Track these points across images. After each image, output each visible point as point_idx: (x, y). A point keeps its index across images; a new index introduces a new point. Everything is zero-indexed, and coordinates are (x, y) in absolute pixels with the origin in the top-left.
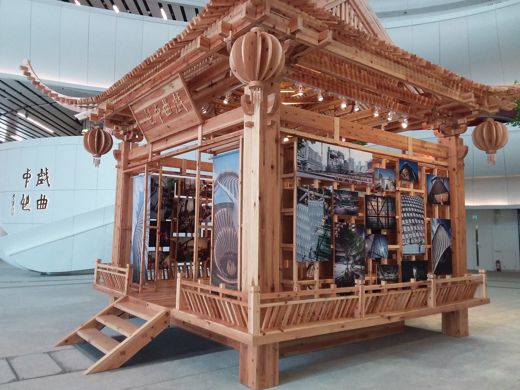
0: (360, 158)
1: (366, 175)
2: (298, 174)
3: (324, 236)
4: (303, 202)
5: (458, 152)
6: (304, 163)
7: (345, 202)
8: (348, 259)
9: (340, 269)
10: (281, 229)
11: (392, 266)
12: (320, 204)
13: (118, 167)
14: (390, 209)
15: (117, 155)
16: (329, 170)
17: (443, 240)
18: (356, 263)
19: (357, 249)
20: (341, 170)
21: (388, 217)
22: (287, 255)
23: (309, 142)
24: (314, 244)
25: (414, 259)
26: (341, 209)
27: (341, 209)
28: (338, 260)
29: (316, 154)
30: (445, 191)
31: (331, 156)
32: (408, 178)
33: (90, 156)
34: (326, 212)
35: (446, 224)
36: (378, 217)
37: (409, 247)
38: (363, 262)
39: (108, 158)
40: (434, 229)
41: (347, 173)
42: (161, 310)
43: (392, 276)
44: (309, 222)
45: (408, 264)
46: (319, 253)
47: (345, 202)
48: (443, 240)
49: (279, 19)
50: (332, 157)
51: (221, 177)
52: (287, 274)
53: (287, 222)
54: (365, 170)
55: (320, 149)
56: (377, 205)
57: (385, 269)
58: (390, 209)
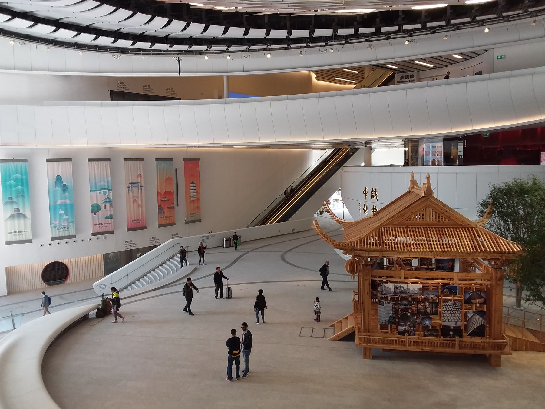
1: (418, 294)
3: (392, 317)
4: (382, 305)
5: (496, 277)
6: (382, 291)
7: (405, 304)
8: (406, 325)
9: (401, 328)
12: (391, 305)
14: (434, 307)
16: (395, 293)
17: (478, 321)
18: (411, 327)
19: (411, 321)
20: (402, 292)
21: (432, 310)
23: (385, 284)
24: (387, 319)
25: (452, 328)
27: (403, 307)
28: (400, 325)
29: (388, 288)
31: (396, 287)
32: (448, 293)
34: (393, 308)
35: (482, 314)
36: (425, 310)
40: (470, 316)
41: (406, 293)
43: (434, 334)
44: (385, 312)
46: (389, 322)
47: (405, 304)
49: (361, 252)
50: (397, 288)
54: (418, 292)
55: (391, 287)
58: (434, 307)
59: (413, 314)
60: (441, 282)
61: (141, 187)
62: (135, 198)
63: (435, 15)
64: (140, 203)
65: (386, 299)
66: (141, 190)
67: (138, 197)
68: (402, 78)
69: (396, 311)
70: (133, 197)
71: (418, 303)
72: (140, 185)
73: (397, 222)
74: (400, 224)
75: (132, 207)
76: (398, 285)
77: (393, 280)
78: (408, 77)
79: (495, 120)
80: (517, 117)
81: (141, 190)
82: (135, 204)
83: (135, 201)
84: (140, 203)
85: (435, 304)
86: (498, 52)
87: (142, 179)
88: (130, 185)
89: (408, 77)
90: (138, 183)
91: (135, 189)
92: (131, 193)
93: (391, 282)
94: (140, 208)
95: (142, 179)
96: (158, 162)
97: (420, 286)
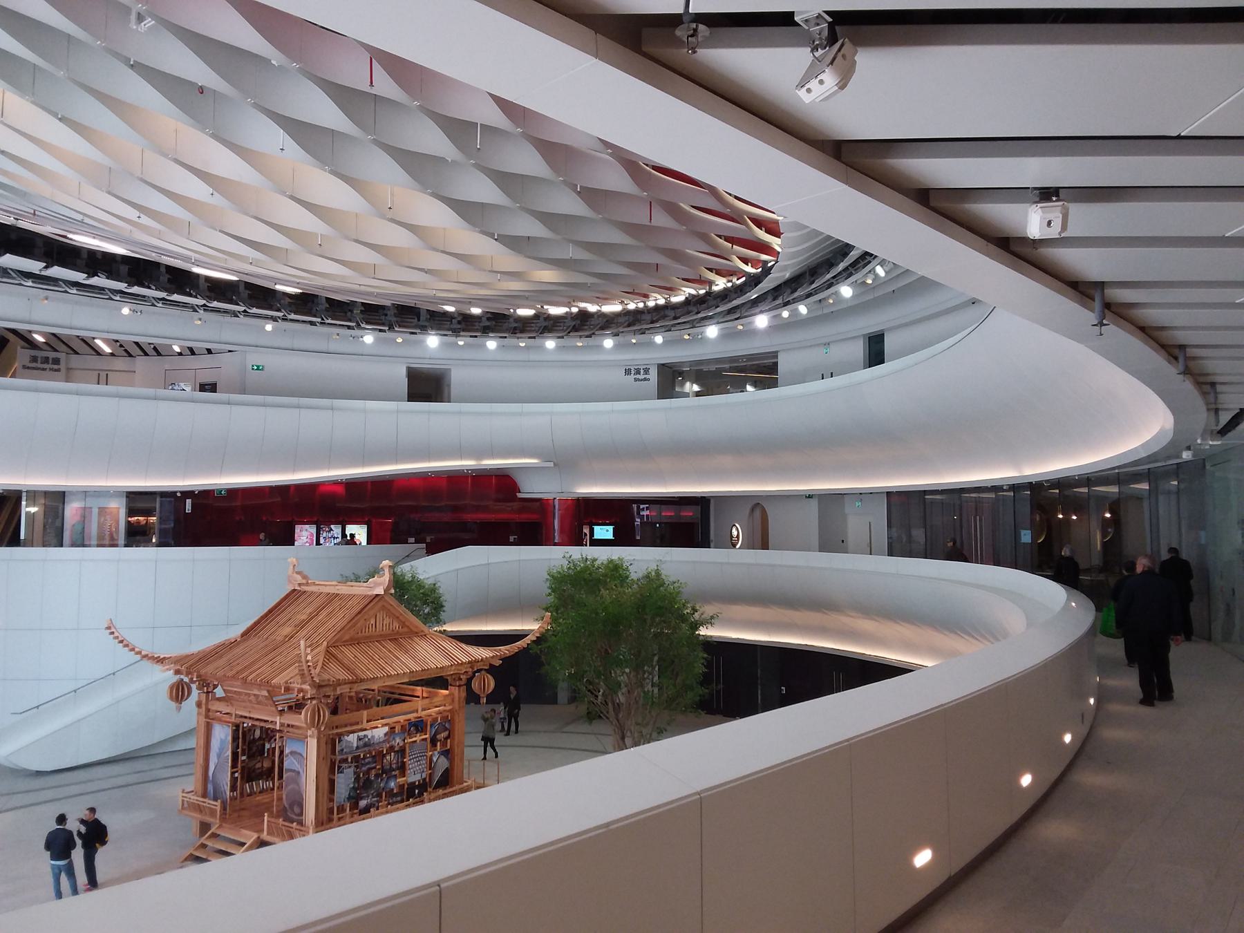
0: (379, 733)
2: (339, 758)
9: (363, 803)
10: (327, 787)
11: (400, 793)
13: (199, 714)
15: (199, 705)
16: (357, 748)
17: (443, 763)
20: (366, 745)
22: (332, 800)
26: (364, 769)
27: (364, 769)
28: (362, 798)
30: (446, 729)
31: (359, 739)
33: (173, 705)
35: (446, 753)
37: (413, 777)
38: (379, 795)
39: (190, 704)
42: (255, 836)
44: (345, 782)
45: (412, 786)
46: (350, 798)
48: (443, 763)
51: (292, 753)
52: (331, 811)
53: (332, 783)
55: (352, 739)
56: (391, 758)
57: (396, 795)
59: (377, 776)
60: (401, 718)
63: (219, 290)
65: (345, 760)
68: (34, 359)
69: (357, 779)
71: (384, 756)
73: (347, 637)
74: (352, 639)
76: (362, 734)
77: (355, 727)
78: (46, 360)
79: (258, 470)
80: (295, 469)
85: (402, 751)
86: (254, 358)
89: (46, 360)
93: (353, 732)
97: (386, 729)
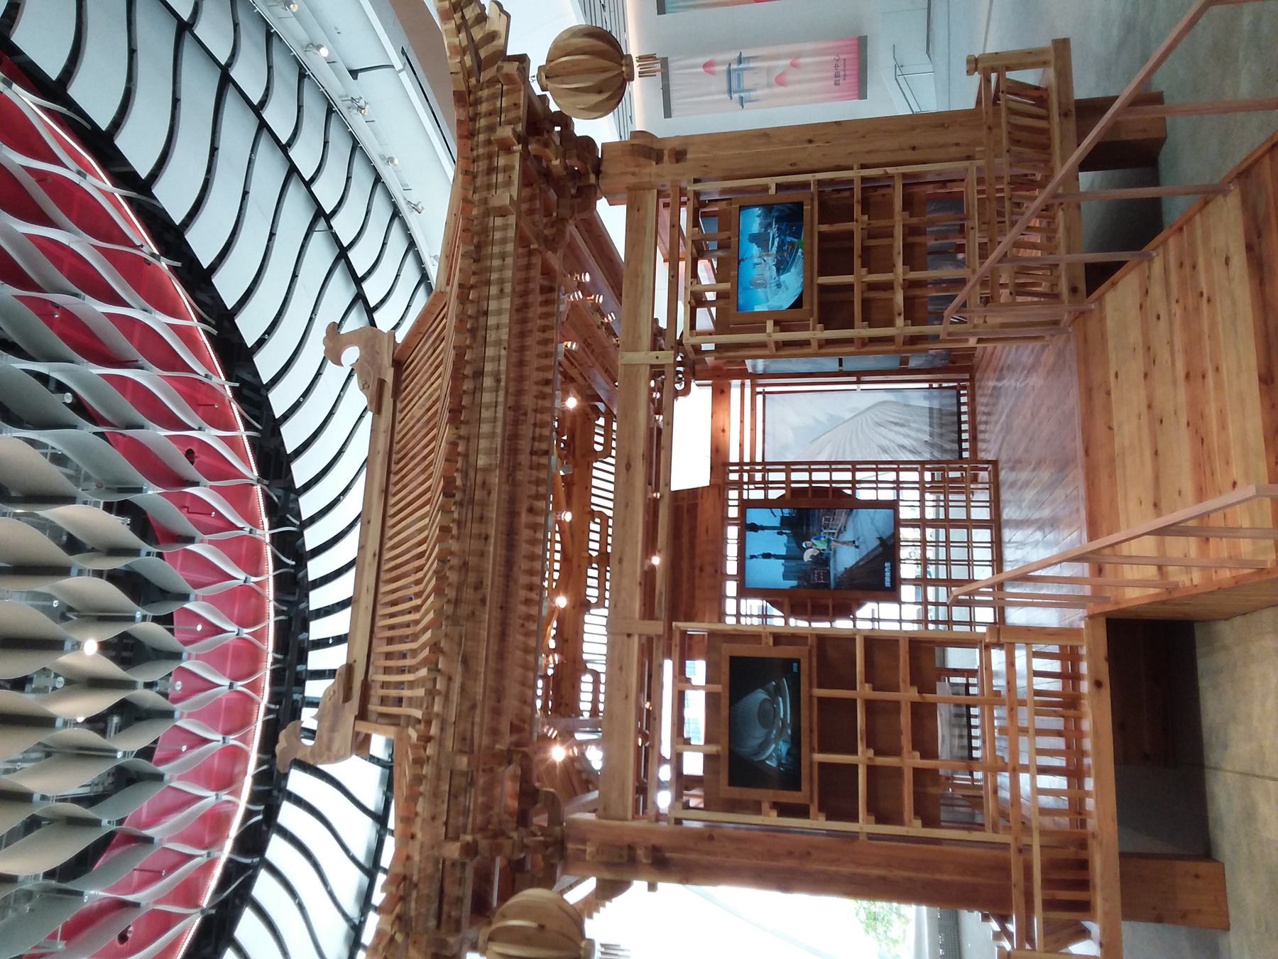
61: (740, 61)
62: (773, 80)
64: (787, 62)
66: (749, 59)
67: (769, 70)
70: (769, 86)
72: (734, 66)
75: (797, 87)
81: (749, 59)
82: (790, 77)
83: (780, 81)
84: (787, 62)
87: (719, 57)
88: (735, 96)
90: (729, 72)
91: (748, 80)
92: (759, 93)
94: (802, 61)
95: (719, 57)
96: (668, 5)
